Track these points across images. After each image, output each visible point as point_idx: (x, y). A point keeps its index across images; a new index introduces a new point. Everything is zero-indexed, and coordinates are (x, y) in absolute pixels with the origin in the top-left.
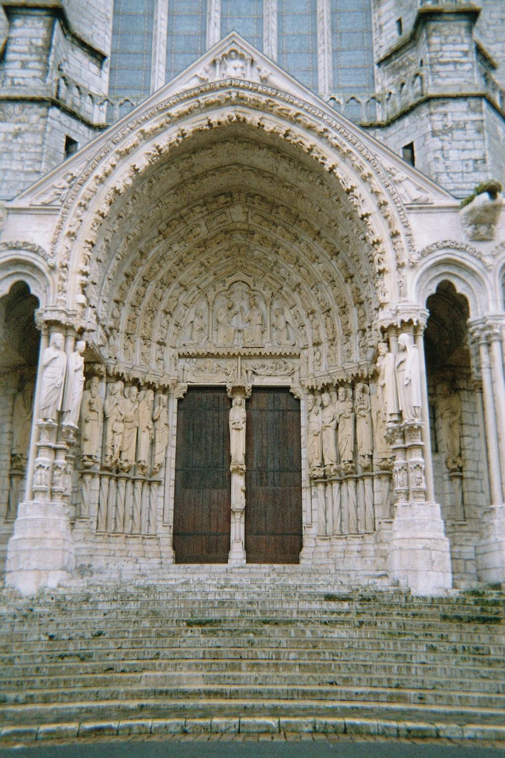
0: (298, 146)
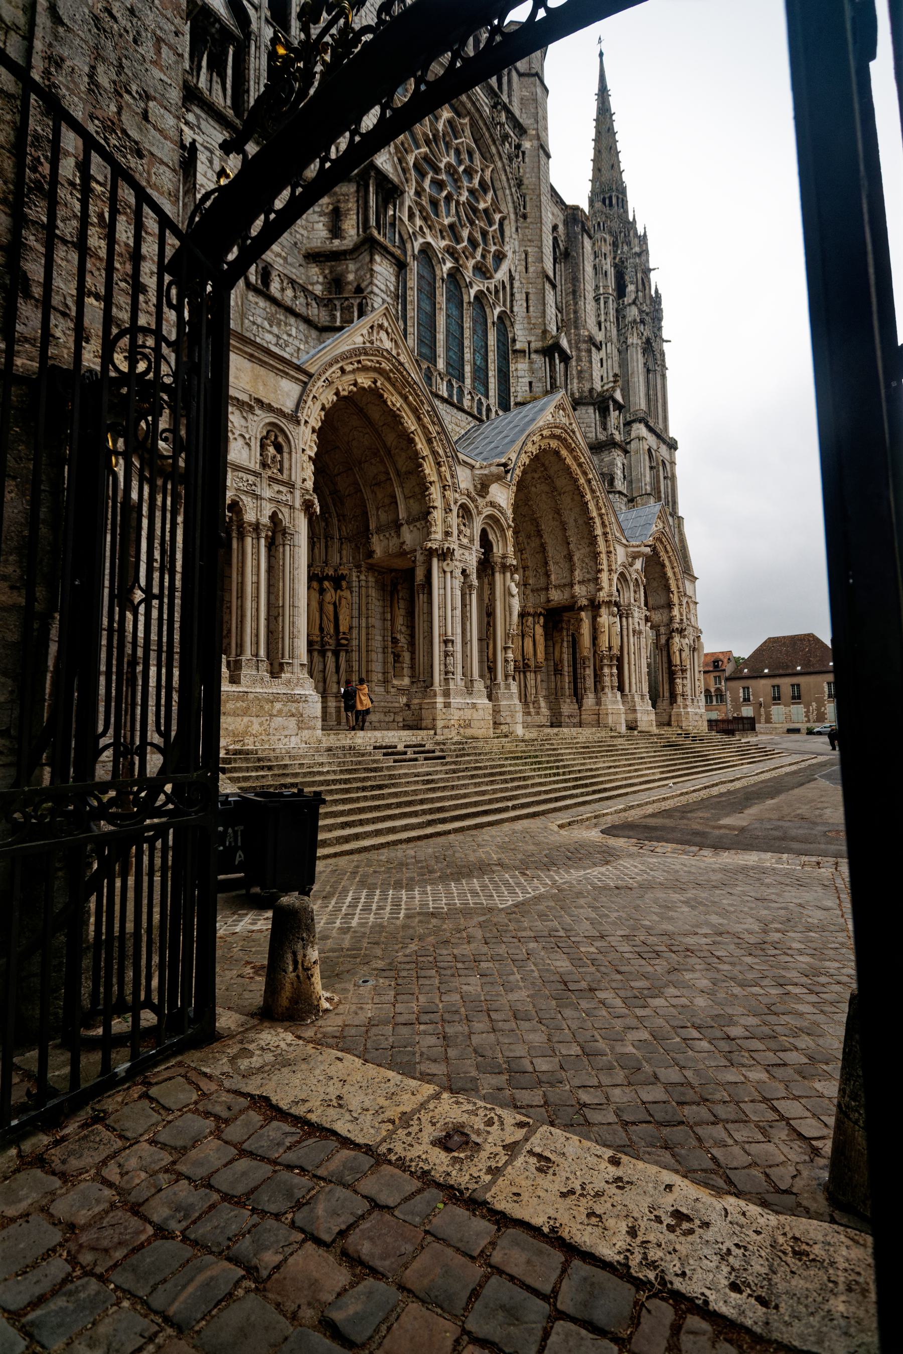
0: (576, 480)
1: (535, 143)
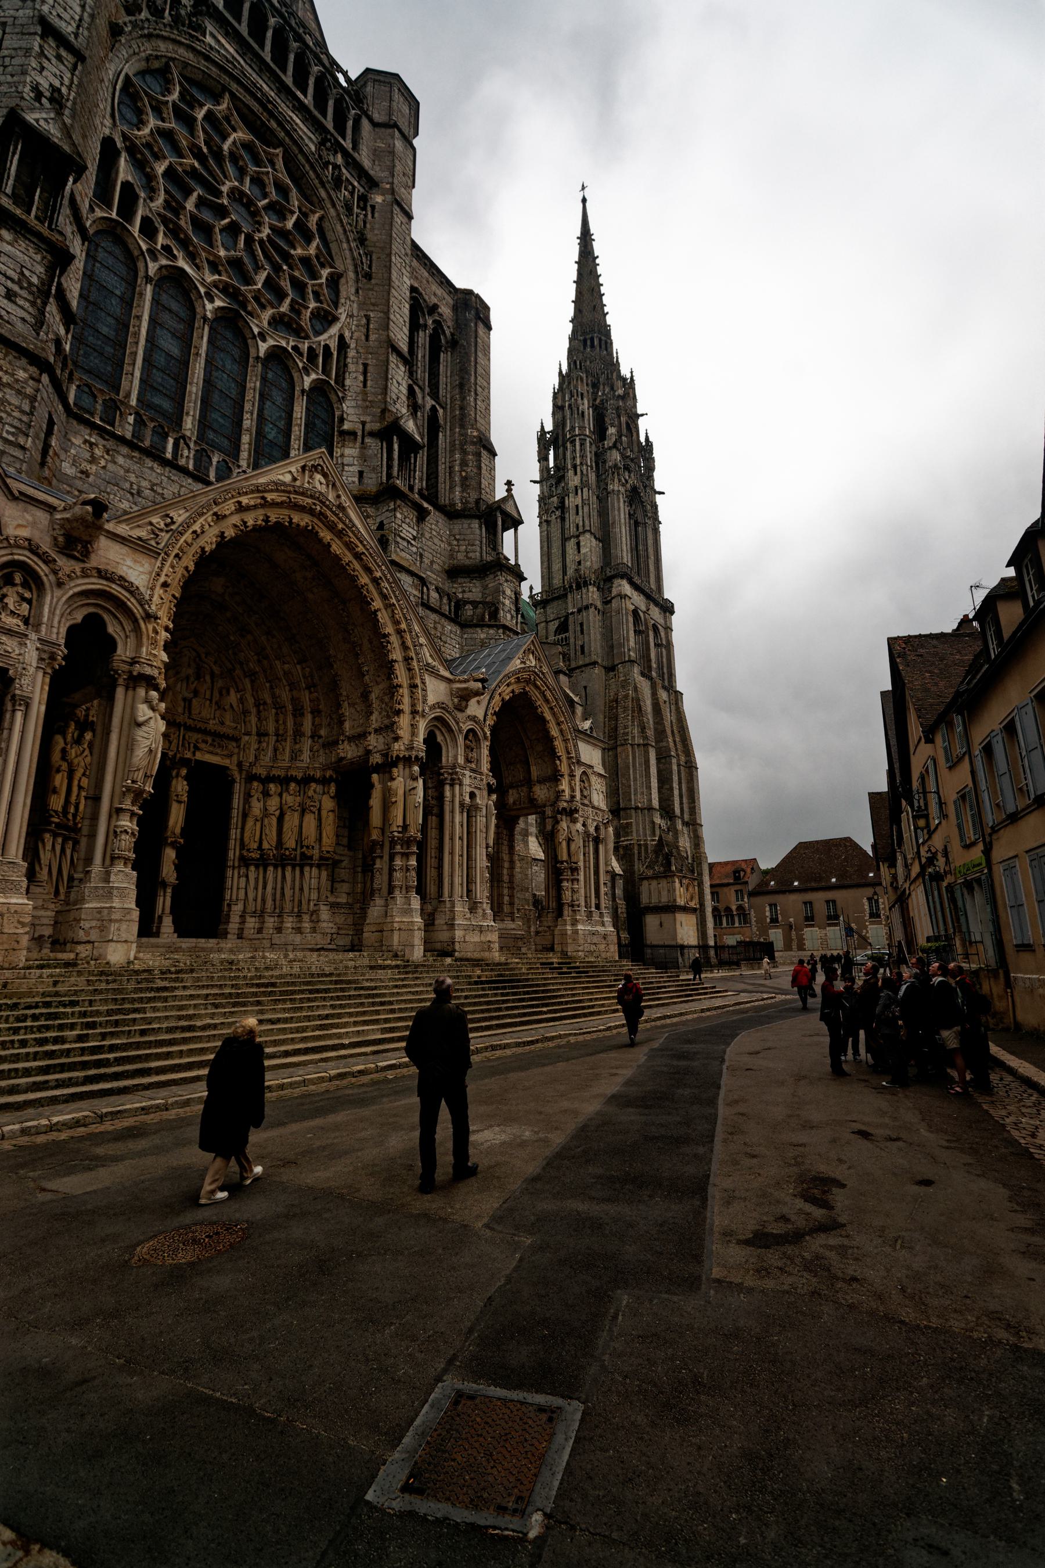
0: (354, 579)
1: (389, 197)
